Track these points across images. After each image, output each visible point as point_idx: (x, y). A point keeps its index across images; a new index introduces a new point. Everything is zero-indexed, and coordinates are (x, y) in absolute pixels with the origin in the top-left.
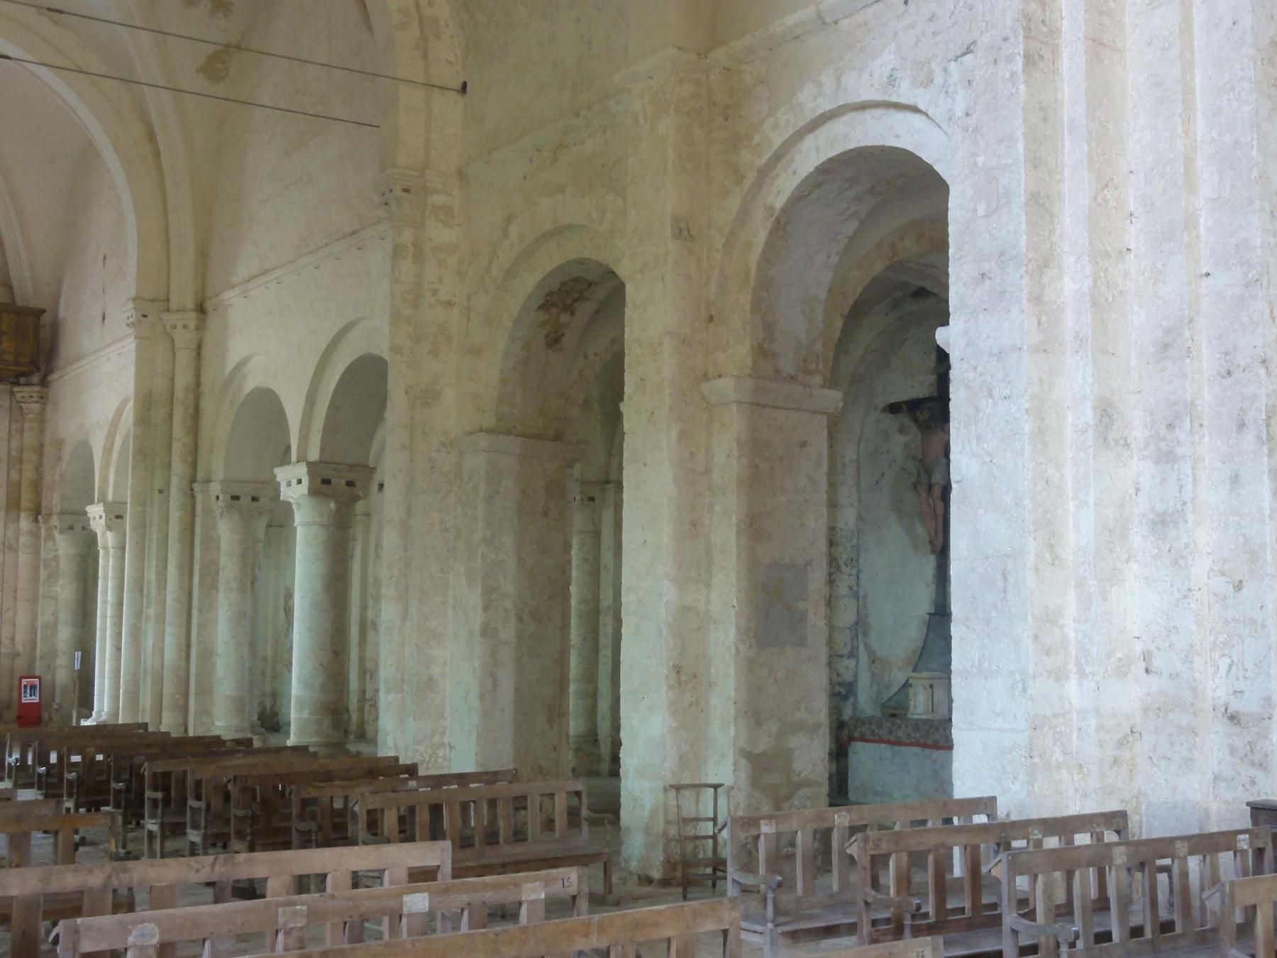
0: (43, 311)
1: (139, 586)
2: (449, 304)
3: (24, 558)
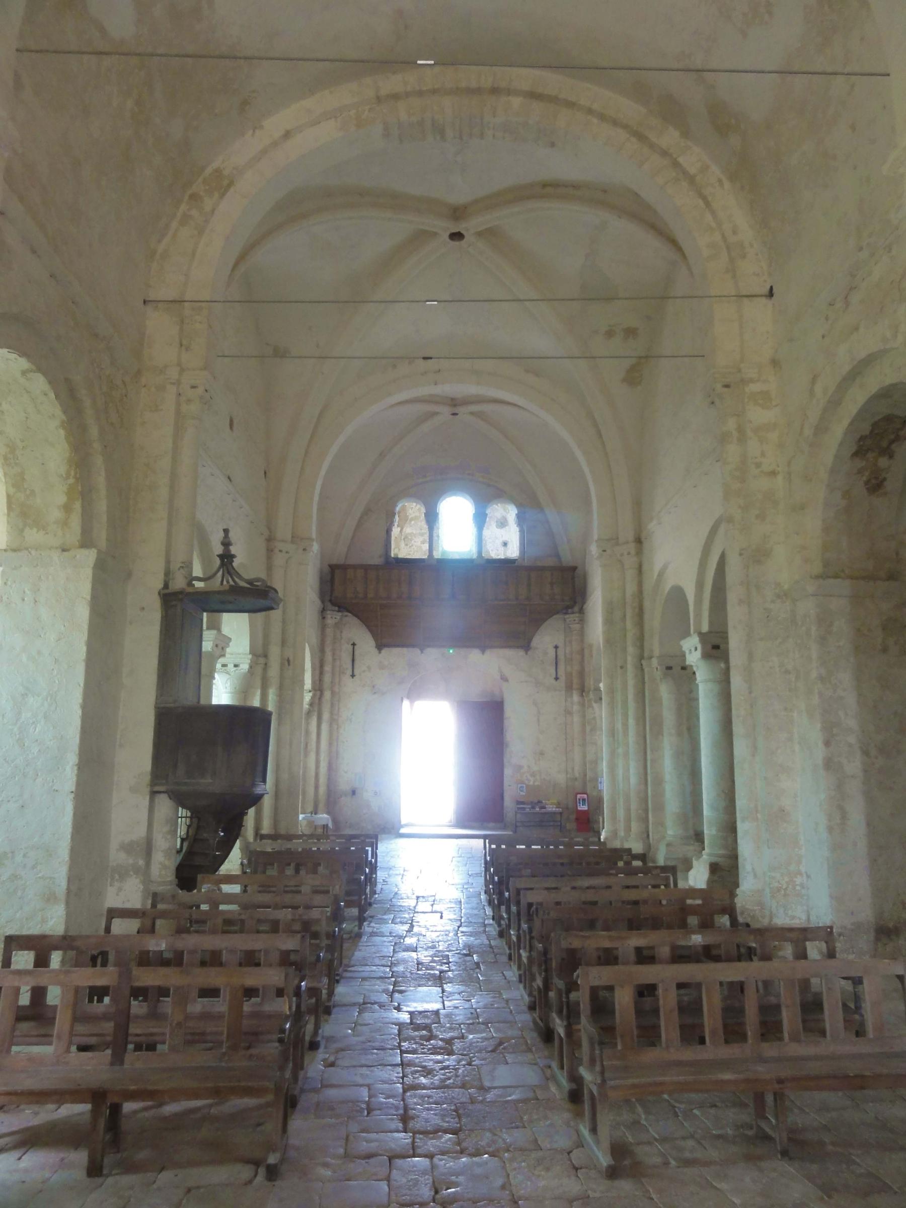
1: (612, 733)
2: (773, 473)
3: (576, 719)
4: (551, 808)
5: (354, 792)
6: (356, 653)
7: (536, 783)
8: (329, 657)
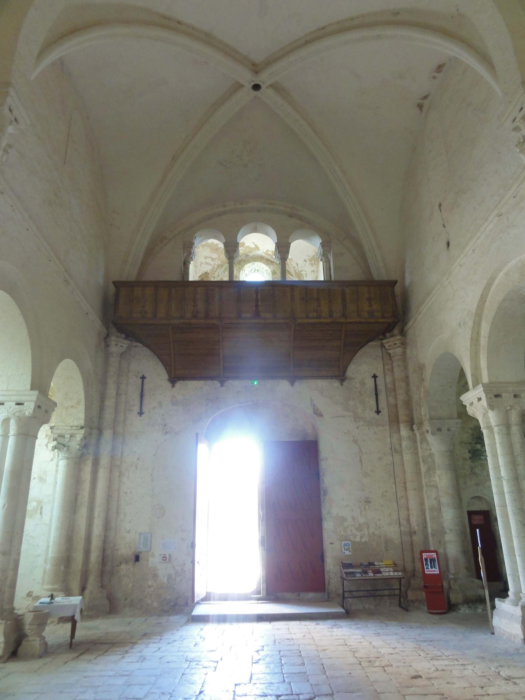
0: (396, 282)
3: (407, 457)
4: (388, 573)
5: (137, 558)
6: (145, 387)
7: (363, 540)
8: (111, 390)
